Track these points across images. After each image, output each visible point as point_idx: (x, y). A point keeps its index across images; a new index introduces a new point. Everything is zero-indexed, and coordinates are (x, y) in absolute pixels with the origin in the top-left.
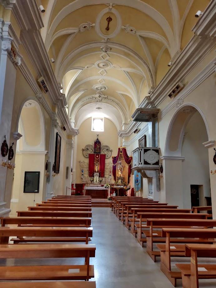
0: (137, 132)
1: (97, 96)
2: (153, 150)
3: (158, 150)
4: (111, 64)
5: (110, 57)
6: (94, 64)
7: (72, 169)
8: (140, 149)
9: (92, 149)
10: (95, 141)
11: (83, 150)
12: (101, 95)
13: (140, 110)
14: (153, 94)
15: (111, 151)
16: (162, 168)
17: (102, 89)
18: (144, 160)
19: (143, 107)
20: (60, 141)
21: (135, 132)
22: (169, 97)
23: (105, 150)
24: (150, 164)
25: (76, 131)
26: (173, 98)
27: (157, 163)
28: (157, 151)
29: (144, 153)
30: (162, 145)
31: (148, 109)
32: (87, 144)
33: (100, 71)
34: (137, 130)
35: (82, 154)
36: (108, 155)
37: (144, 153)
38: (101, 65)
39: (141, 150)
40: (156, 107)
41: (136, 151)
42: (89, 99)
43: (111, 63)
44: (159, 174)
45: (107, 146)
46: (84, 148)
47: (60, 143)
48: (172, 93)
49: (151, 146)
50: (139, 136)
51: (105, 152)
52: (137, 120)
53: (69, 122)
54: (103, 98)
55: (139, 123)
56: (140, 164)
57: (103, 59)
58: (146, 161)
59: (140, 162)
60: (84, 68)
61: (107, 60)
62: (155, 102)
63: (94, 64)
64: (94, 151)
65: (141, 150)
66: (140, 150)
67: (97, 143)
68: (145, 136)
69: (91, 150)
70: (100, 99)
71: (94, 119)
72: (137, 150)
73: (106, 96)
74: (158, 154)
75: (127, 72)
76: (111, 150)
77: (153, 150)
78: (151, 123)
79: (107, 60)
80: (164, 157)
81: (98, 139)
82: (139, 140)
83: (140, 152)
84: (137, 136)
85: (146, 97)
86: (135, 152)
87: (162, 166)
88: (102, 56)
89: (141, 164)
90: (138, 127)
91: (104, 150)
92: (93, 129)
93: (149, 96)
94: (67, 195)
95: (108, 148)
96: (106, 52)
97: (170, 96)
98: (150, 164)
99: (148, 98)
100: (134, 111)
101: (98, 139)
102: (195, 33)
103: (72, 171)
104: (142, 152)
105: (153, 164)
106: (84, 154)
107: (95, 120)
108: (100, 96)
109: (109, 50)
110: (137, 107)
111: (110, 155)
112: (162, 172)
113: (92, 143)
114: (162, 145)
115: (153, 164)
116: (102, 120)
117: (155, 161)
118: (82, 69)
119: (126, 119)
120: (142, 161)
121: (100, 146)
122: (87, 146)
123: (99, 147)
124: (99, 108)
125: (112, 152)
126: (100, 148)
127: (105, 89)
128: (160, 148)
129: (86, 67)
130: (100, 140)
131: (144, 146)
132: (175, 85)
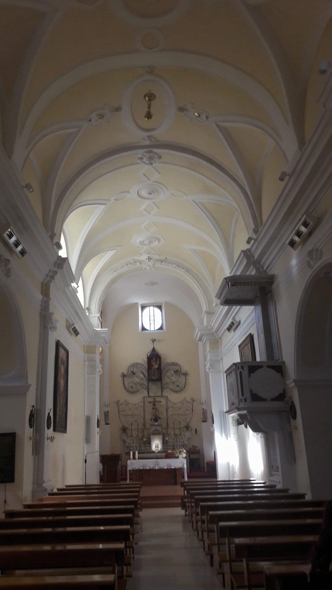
0: (234, 327)
1: (144, 257)
2: (268, 367)
3: (281, 366)
4: (165, 189)
5: (159, 173)
6: (129, 192)
7: (98, 421)
8: (240, 367)
9: (143, 373)
11: (124, 376)
12: (151, 256)
13: (232, 282)
14: (256, 244)
15: (186, 374)
16: (292, 407)
17: (151, 242)
18: (251, 391)
19: (238, 274)
20: (65, 359)
21: (229, 329)
22: (289, 247)
23: (173, 372)
24: (265, 400)
25: (104, 335)
26: (300, 247)
27: (281, 397)
28: (280, 369)
29: (250, 376)
30: (288, 354)
31: (250, 277)
32: (132, 363)
33: (143, 207)
34: (233, 323)
36: (178, 383)
37: (250, 376)
38: (144, 193)
39: (242, 368)
40: (265, 271)
41: (231, 372)
42: (127, 265)
43: (166, 188)
44: (290, 423)
45: (174, 364)
47: (66, 364)
48: (296, 239)
49: (264, 359)
50: (237, 337)
52: (228, 302)
53: (87, 318)
54: (158, 260)
55: (236, 308)
56: (243, 401)
57: (147, 180)
58: (256, 394)
59: (243, 395)
60: (109, 200)
61: (155, 182)
62: (263, 260)
63: (129, 192)
64: (146, 374)
65: (242, 368)
66: (240, 370)
67: (154, 357)
68: (251, 337)
69: (142, 376)
70: (151, 263)
71: (143, 308)
72: (232, 369)
73: (163, 258)
74: (282, 375)
75: (201, 203)
76: (183, 371)
77: (268, 367)
78: (259, 308)
79: (155, 182)
80: (295, 381)
81: (154, 349)
82: (239, 346)
83: (241, 373)
84: (234, 339)
85: (242, 251)
86: (229, 374)
87: (293, 402)
88: (144, 174)
89: (245, 400)
90: (234, 317)
91: (169, 373)
92: (144, 329)
93: (249, 250)
94: (87, 483)
95: (178, 368)
96: (151, 164)
97: (292, 244)
98: (265, 400)
99: (247, 254)
100: (219, 282)
101: (154, 349)
102: (325, 106)
103: (98, 427)
104: (245, 372)
105: (273, 400)
107: (147, 310)
108: (149, 259)
109: (157, 160)
110: (228, 274)
112: (295, 417)
114: (288, 354)
115: (273, 400)
116: (160, 307)
117: (276, 394)
118: (105, 204)
119: (210, 302)
120: (247, 395)
121: (160, 364)
123: (156, 366)
124: (153, 284)
125: (188, 377)
126: (159, 369)
127: (159, 241)
128: (284, 362)
129: (113, 199)
130: (161, 349)
131: (250, 360)
132: (300, 220)
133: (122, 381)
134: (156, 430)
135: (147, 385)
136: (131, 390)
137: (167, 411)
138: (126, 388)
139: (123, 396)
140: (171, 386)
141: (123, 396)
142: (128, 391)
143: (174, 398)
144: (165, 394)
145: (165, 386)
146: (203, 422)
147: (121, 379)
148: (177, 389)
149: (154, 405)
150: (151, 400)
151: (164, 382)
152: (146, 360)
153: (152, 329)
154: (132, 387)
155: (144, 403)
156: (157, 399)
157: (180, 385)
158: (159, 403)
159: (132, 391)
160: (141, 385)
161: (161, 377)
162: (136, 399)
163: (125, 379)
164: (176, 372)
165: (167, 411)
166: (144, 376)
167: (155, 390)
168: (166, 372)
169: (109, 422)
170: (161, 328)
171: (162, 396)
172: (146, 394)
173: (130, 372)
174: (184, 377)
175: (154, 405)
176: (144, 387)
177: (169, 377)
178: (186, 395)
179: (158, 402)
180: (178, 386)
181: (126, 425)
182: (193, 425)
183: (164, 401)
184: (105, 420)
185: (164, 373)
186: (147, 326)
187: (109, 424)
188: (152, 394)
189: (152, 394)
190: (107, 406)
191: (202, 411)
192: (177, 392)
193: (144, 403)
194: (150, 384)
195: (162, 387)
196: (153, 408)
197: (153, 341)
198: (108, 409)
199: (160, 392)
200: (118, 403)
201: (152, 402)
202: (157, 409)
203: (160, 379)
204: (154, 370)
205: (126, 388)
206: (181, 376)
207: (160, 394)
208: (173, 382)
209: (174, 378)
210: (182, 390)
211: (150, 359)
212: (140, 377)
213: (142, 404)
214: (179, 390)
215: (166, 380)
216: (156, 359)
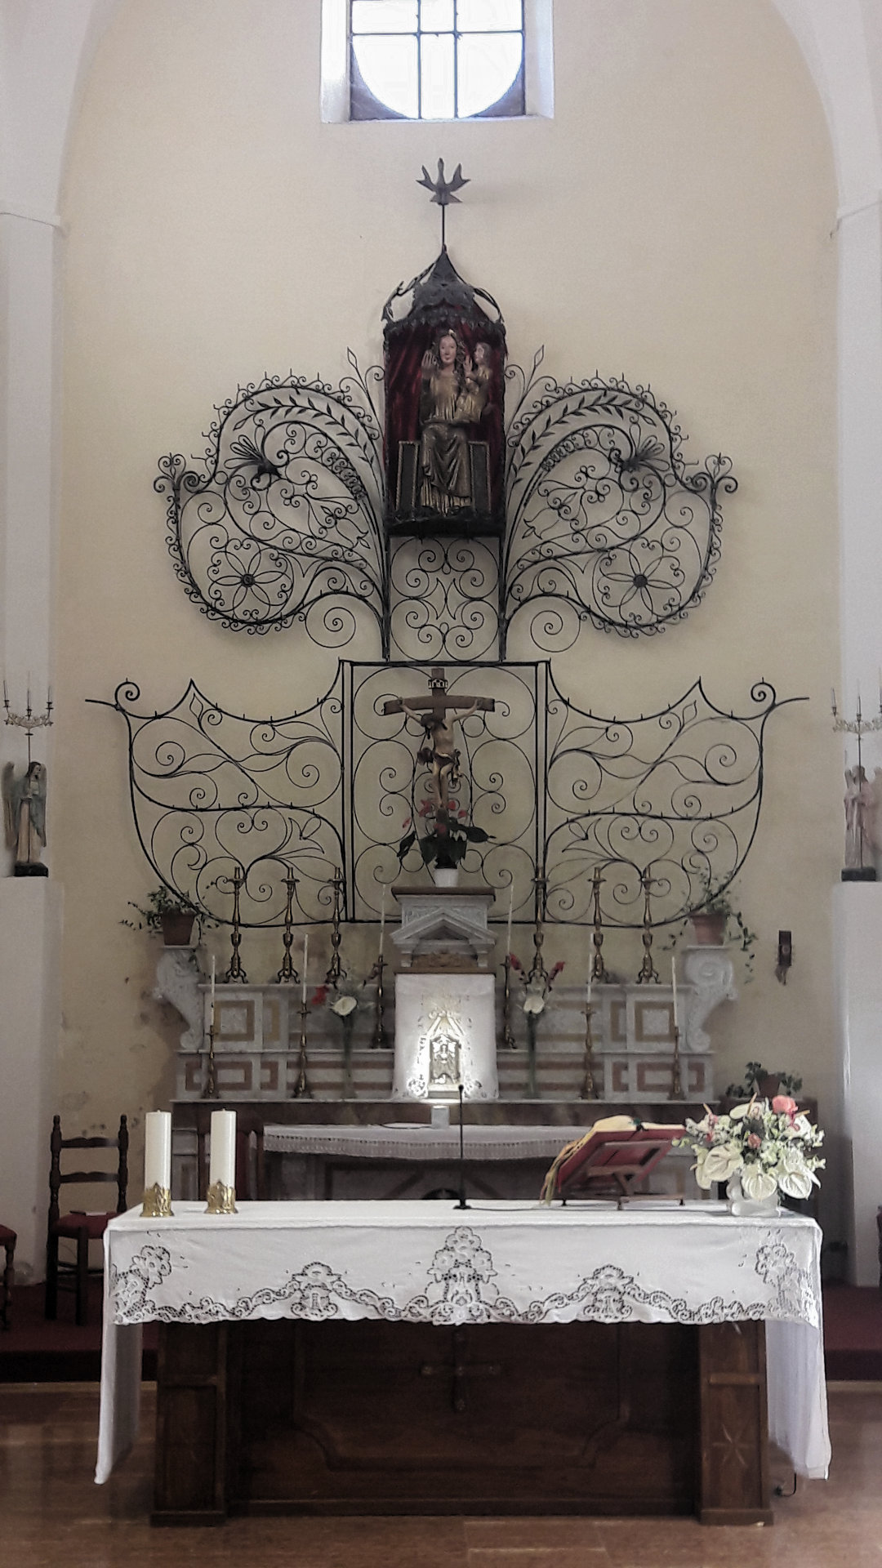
9: (340, 466)
10: (402, 308)
11: (180, 485)
15: (712, 486)
23: (602, 468)
35: (166, 561)
36: (645, 560)
46: (194, 453)
51: (597, 514)
64: (372, 478)
69: (331, 486)
76: (696, 454)
81: (444, 267)
91: (566, 473)
92: (360, 106)
95: (647, 433)
101: (444, 267)
106: (200, 555)
111: (692, 569)
113: (340, 345)
121: (495, 392)
122: (259, 400)
126: (488, 427)
133: (166, 531)
134: (444, 932)
135: (374, 567)
136: (245, 604)
137: (541, 787)
138: (194, 590)
139: (171, 650)
140: (586, 582)
141: (171, 650)
142: (211, 609)
143: (604, 676)
144: (521, 646)
145: (527, 584)
146: (848, 876)
147: (157, 508)
148: (636, 607)
149: (433, 724)
150: (414, 686)
151: (520, 547)
152: (372, 353)
153: (438, 109)
154: (248, 581)
155: (348, 709)
156: (461, 685)
157: (663, 572)
158: (473, 724)
159: (244, 614)
160: (327, 562)
161: (500, 501)
162: (284, 677)
163: (193, 514)
164: (632, 463)
165: (541, 787)
166: (358, 490)
167: (442, 609)
168: (547, 464)
169: (44, 858)
170: (515, 104)
171: (501, 664)
172: (365, 642)
173: (229, 458)
174: (700, 511)
175: (433, 724)
176: (355, 582)
177: (568, 507)
178: (714, 654)
179: (465, 703)
180: (641, 581)
181: (184, 882)
182: (762, 906)
183: (513, 697)
184: (13, 843)
185: (526, 474)
186: (387, 85)
187: (40, 871)
188: (410, 645)
189: (410, 645)
190: (26, 722)
191: (845, 789)
192: (629, 629)
193: (348, 709)
194: (405, 564)
195: (504, 592)
196: (425, 756)
197: (444, 192)
198: (42, 748)
199: (491, 625)
200: (122, 702)
201: (416, 704)
202: (453, 760)
203: (482, 524)
204: (440, 447)
205: (194, 590)
206: (678, 500)
207: (482, 645)
208: (605, 553)
209: (610, 517)
210: (677, 612)
211: (407, 343)
212: (321, 503)
213: (329, 721)
214: (649, 614)
215: (538, 525)
216: (468, 343)
